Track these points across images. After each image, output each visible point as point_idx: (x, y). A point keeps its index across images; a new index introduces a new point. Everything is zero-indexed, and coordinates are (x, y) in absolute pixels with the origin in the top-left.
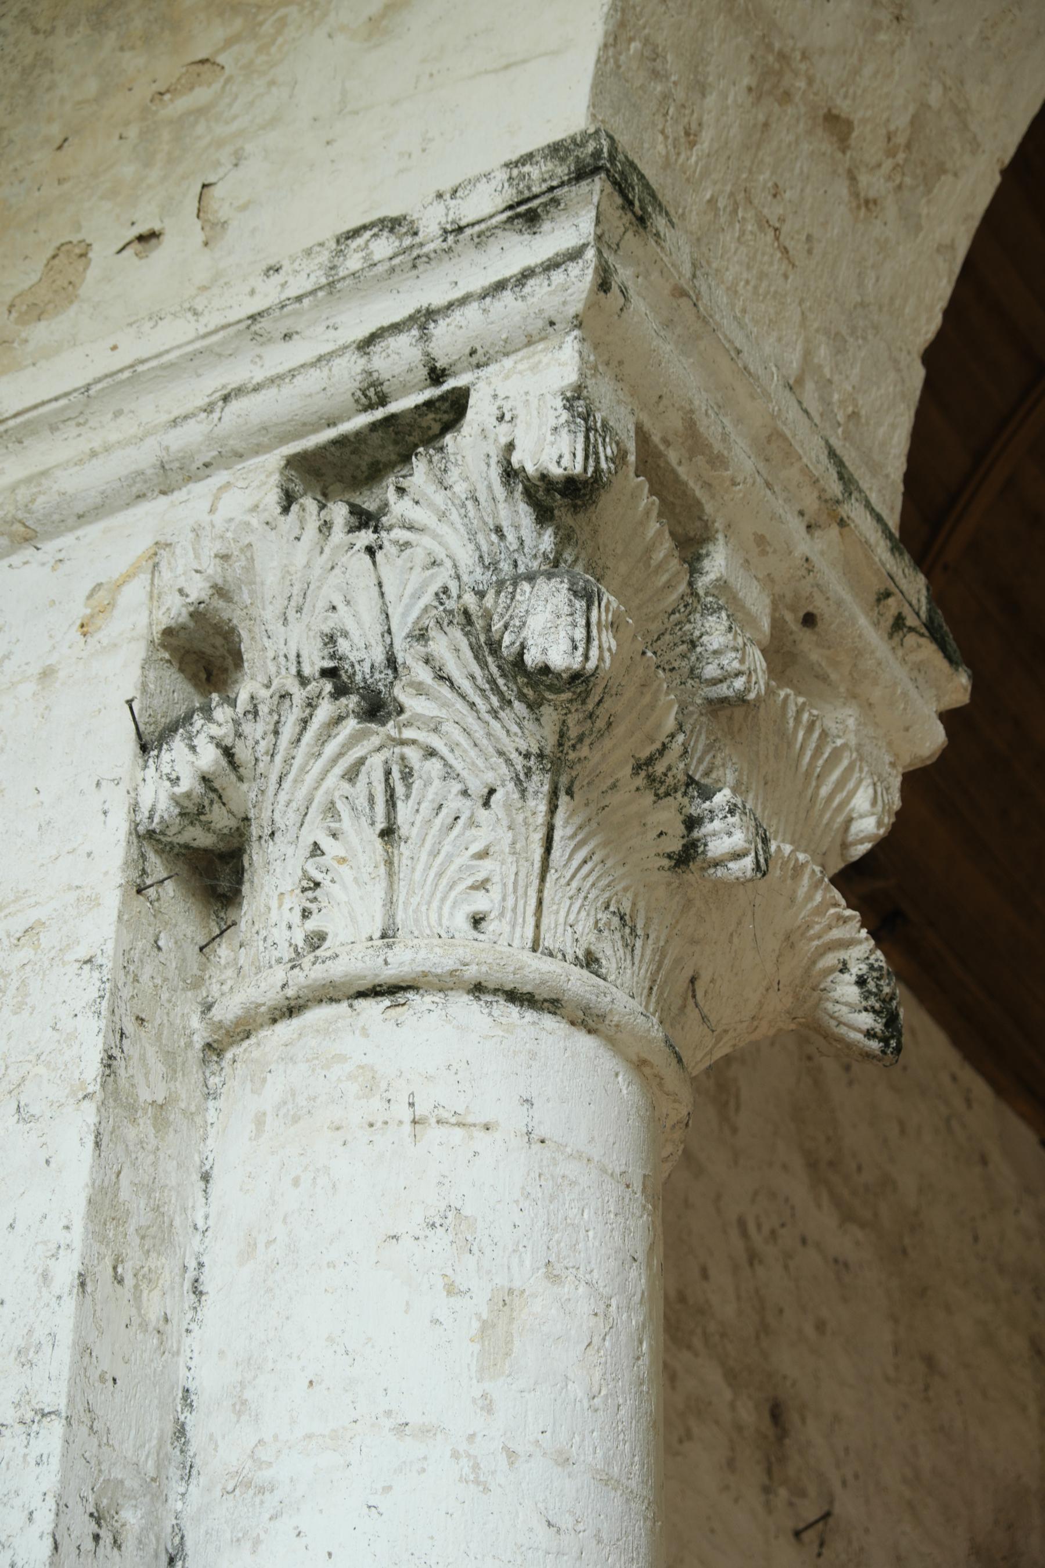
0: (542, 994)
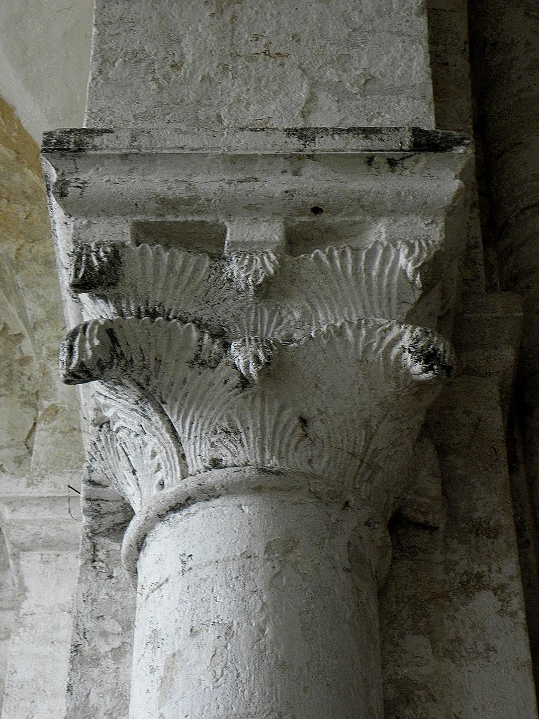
0: (183, 501)
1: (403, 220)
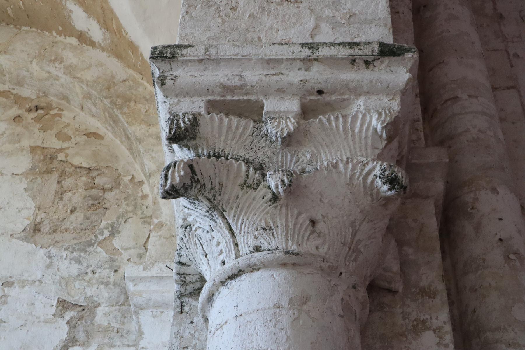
0: (236, 272)
1: (374, 98)
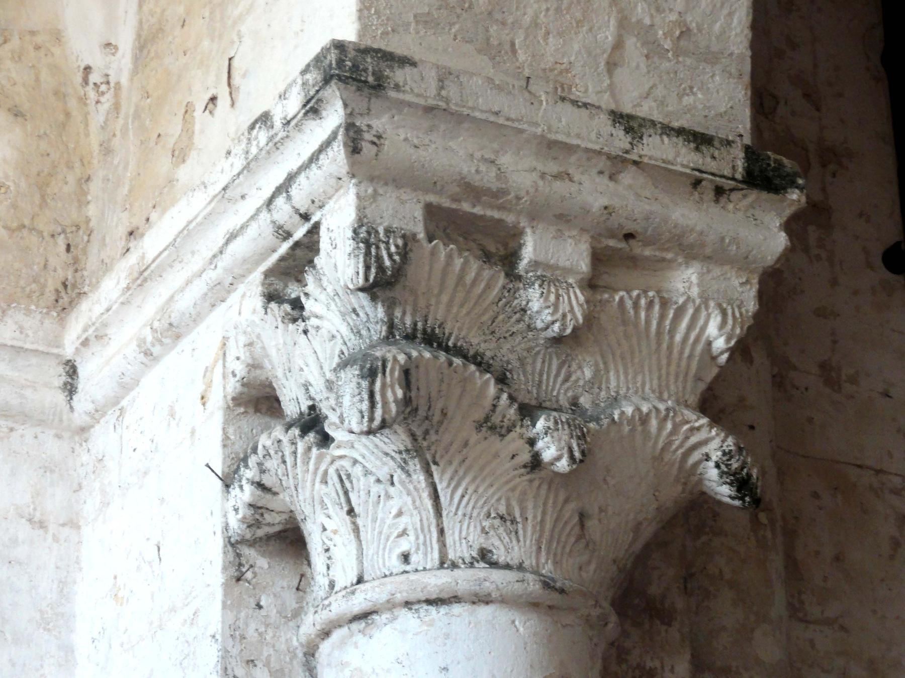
0: (444, 596)
1: (717, 271)
